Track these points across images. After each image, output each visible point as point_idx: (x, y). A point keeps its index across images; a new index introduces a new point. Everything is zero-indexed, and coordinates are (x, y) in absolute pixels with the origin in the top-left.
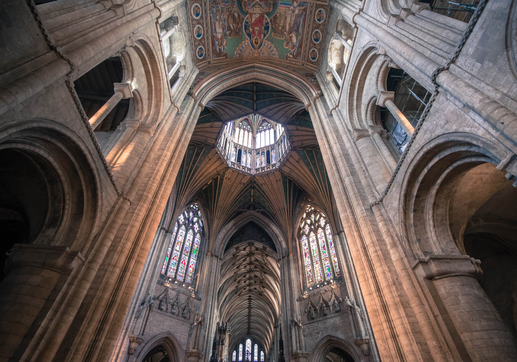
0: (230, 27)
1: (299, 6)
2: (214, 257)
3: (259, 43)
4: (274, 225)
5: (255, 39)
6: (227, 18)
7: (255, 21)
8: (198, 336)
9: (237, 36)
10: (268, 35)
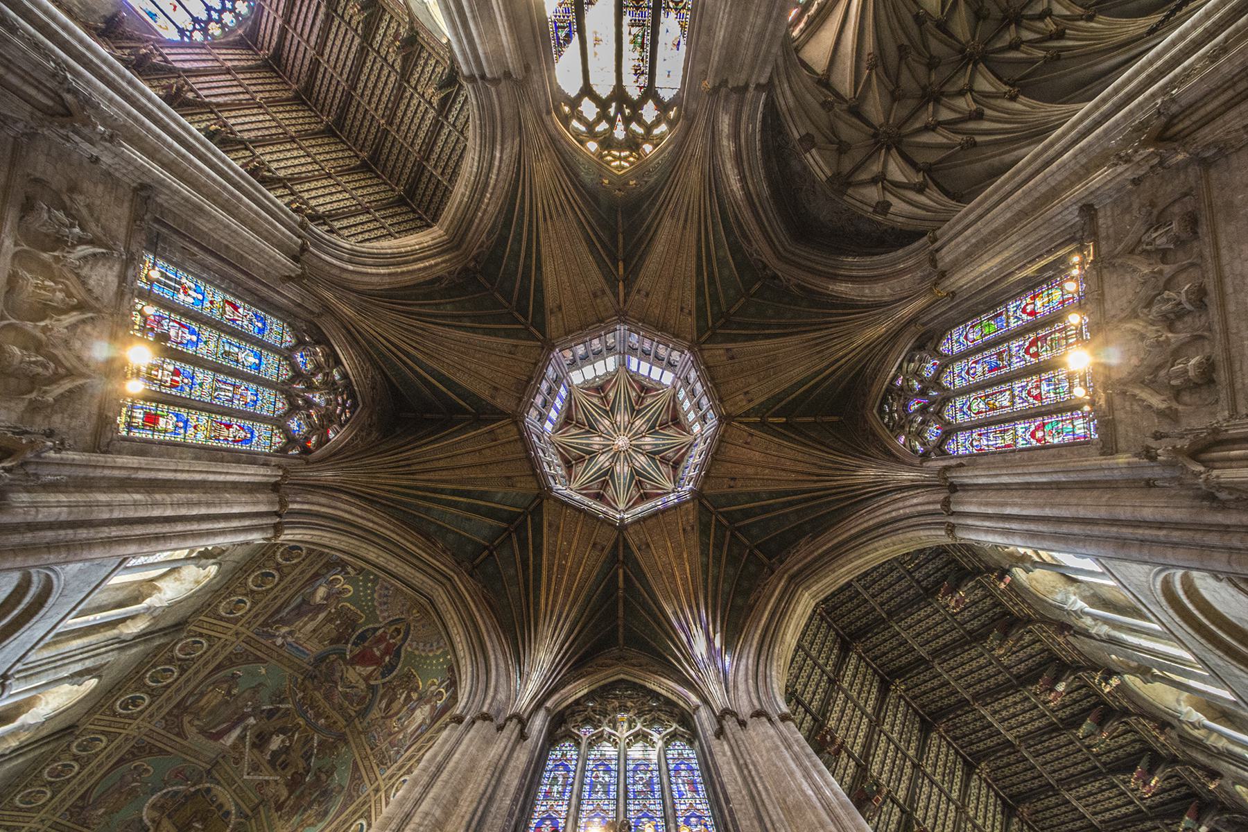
0: (405, 700)
1: (274, 636)
2: (940, 265)
4: (732, 191)
8: (1231, 93)
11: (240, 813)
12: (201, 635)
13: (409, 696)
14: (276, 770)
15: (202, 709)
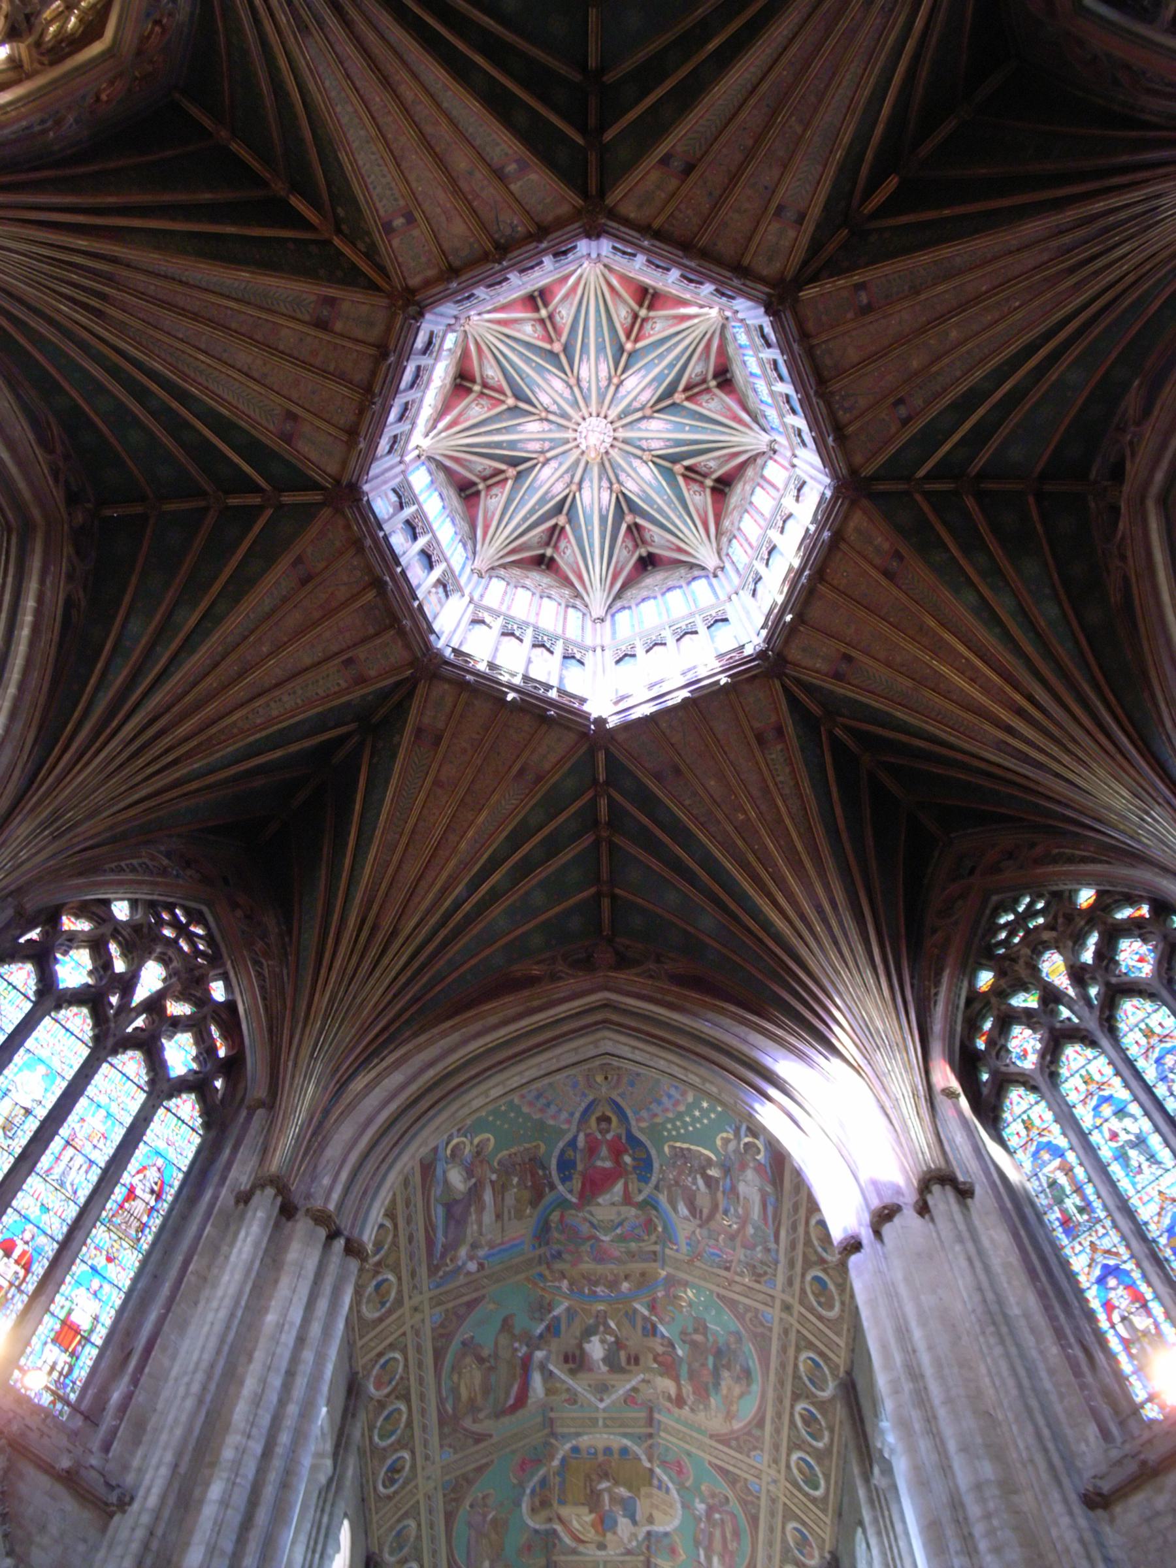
1: (458, 1270)
3: (593, 1122)
5: (608, 1131)
6: (718, 1216)
7: (614, 1183)
9: (681, 1149)
10: (561, 1145)
11: (639, 1439)
12: (380, 1355)
13: (709, 1181)
14: (630, 1372)
15: (472, 1400)
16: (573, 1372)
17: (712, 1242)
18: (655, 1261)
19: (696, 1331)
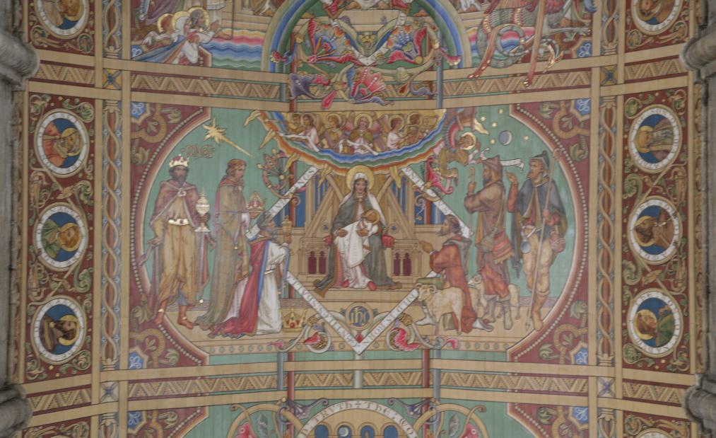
1: (173, 46)
14: (398, 286)
16: (320, 288)
17: (506, 26)
18: (431, 97)
19: (487, 182)
